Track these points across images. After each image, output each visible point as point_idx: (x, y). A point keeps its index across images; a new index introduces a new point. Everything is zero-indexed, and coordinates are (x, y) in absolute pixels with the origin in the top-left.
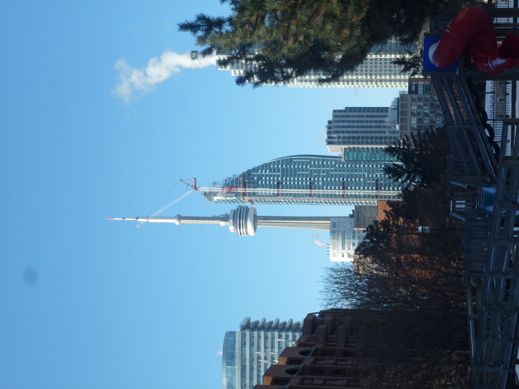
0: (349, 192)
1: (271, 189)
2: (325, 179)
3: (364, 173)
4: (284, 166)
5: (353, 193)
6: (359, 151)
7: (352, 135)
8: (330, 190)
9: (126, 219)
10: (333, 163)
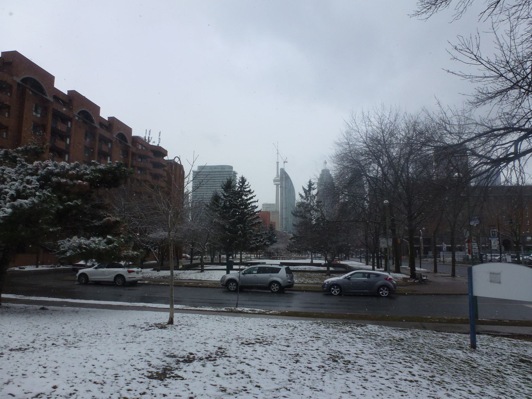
0: (284, 210)
5: (284, 211)
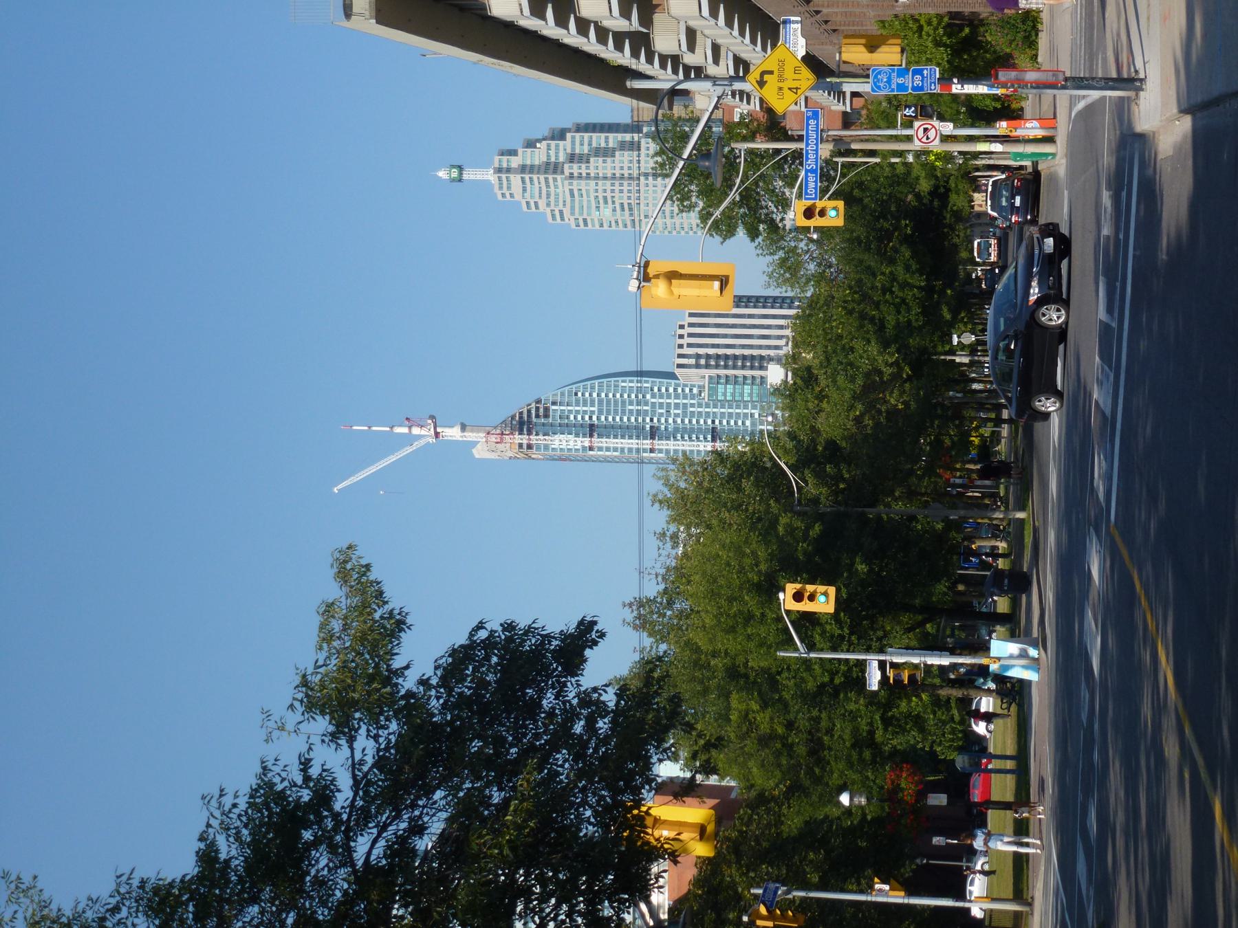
1: (577, 439)
2: (679, 421)
3: (753, 411)
4: (603, 395)
6: (736, 383)
7: (721, 351)
8: (688, 443)
9: (374, 428)
10: (695, 391)
